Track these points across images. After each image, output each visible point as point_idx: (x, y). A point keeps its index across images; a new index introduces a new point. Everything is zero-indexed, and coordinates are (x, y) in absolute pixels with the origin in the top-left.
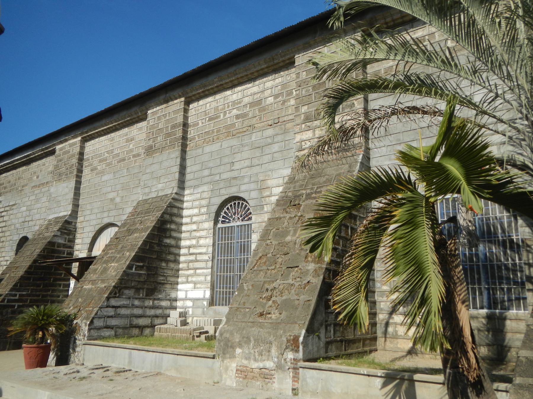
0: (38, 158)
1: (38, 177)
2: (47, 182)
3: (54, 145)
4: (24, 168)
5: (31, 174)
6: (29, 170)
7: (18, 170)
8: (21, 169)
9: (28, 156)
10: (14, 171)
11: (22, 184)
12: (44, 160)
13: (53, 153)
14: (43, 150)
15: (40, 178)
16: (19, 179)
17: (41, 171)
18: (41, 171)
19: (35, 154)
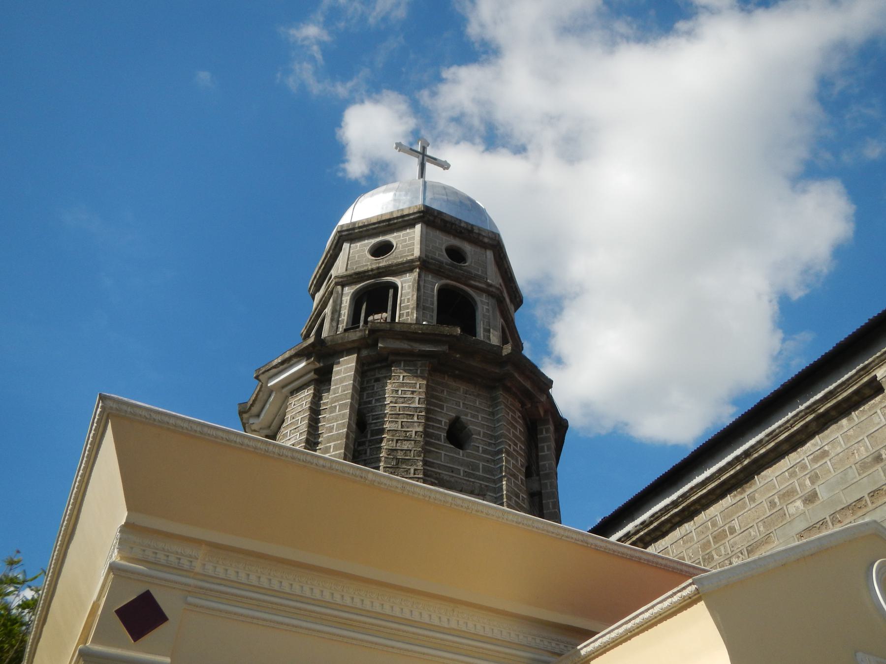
0: (785, 447)
1: (811, 498)
2: (873, 494)
3: (866, 370)
4: (728, 500)
5: (772, 504)
6: (752, 499)
7: (702, 517)
8: (714, 510)
9: (747, 454)
10: (687, 527)
11: (743, 545)
12: (810, 447)
13: (875, 388)
14: (810, 409)
15: (823, 494)
16: (719, 537)
17: (814, 479)
18: (814, 479)
19: (777, 435)
